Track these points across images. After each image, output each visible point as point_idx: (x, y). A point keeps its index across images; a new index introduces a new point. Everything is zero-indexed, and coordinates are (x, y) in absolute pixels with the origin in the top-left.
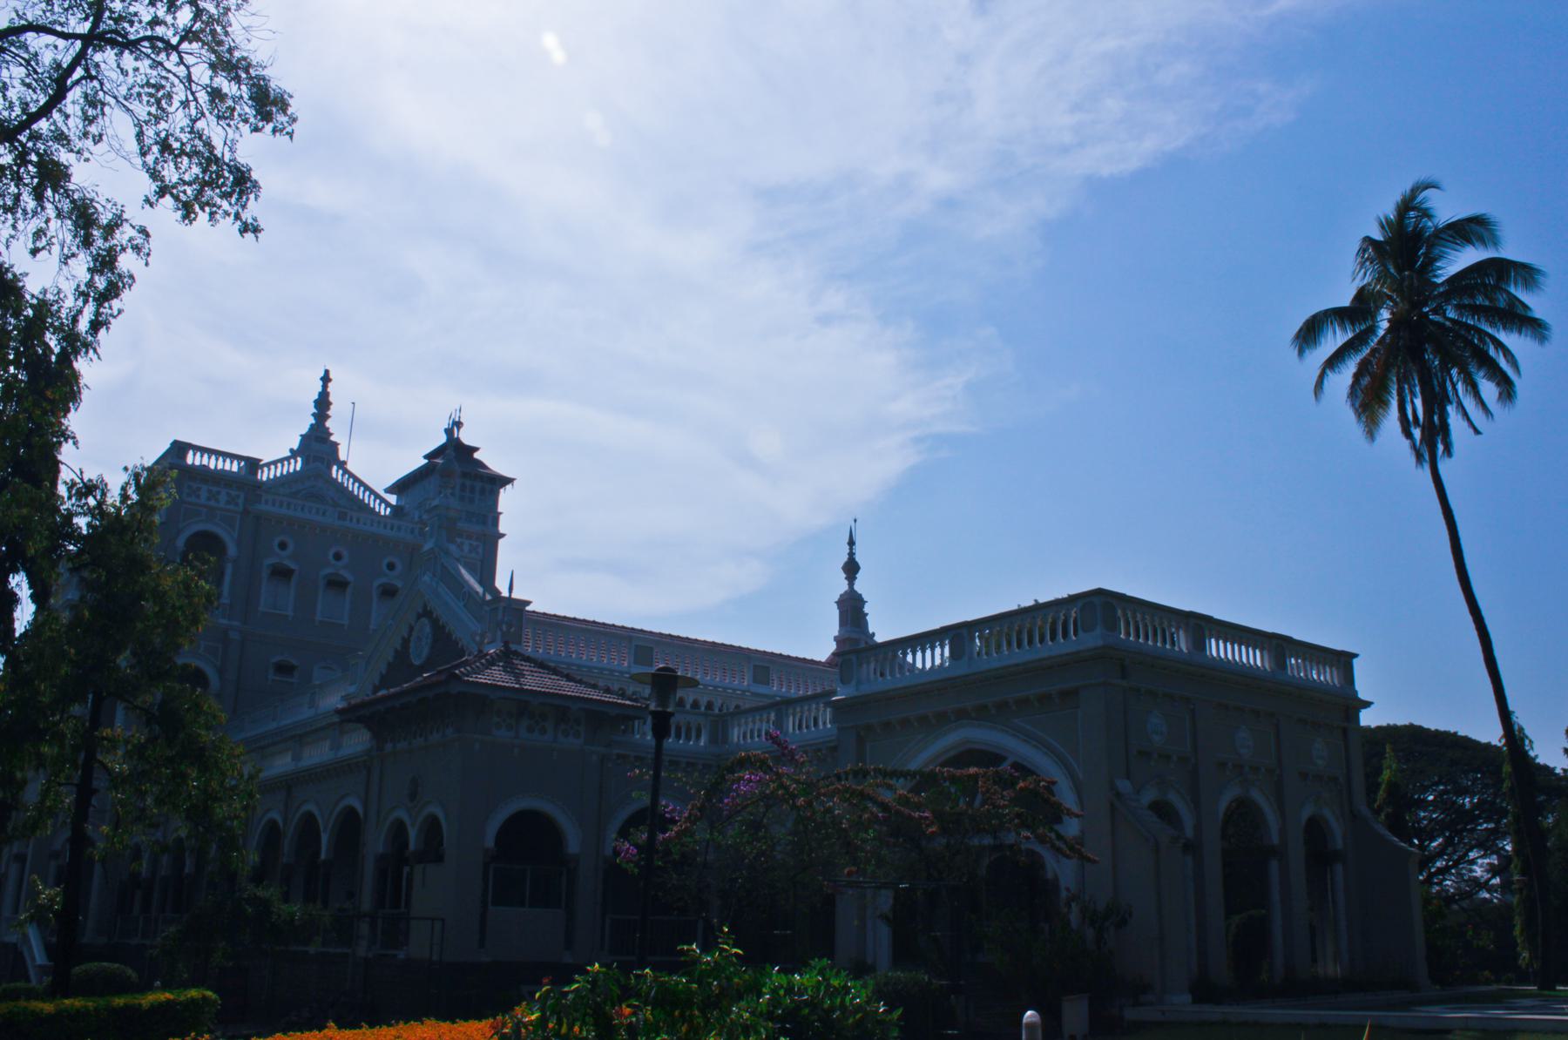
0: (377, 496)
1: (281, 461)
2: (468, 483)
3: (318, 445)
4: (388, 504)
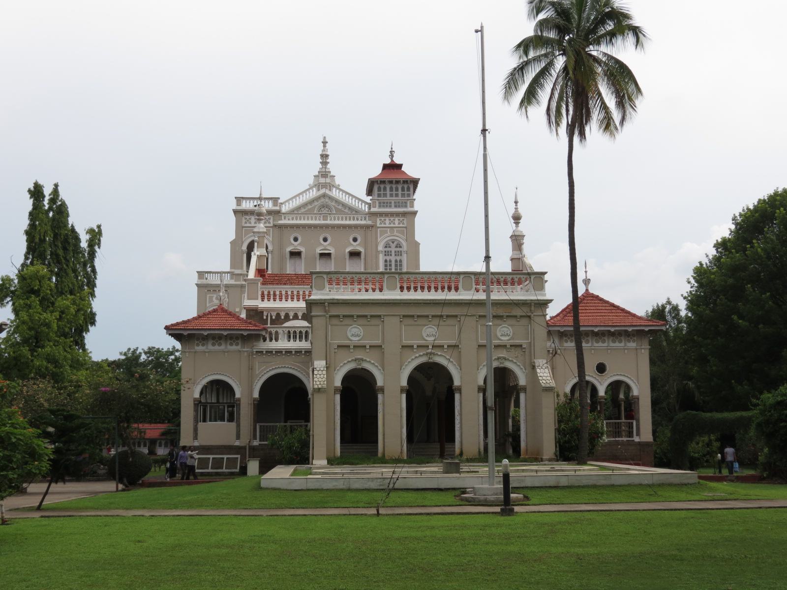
0: (359, 200)
1: (305, 191)
2: (394, 186)
3: (324, 177)
4: (366, 203)
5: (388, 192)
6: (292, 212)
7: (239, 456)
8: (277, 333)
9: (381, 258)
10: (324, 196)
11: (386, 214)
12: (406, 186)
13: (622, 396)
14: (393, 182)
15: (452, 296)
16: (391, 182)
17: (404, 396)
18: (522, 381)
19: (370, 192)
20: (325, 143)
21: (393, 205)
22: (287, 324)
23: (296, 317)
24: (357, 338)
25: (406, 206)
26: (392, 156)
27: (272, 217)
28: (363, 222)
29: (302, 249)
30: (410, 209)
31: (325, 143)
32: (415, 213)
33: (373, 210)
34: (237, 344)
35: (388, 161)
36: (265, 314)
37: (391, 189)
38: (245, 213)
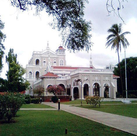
9: (60, 63)
10: (48, 51)
15: (89, 72)
18: (109, 86)
19: (56, 51)
28: (56, 57)
38: (35, 54)
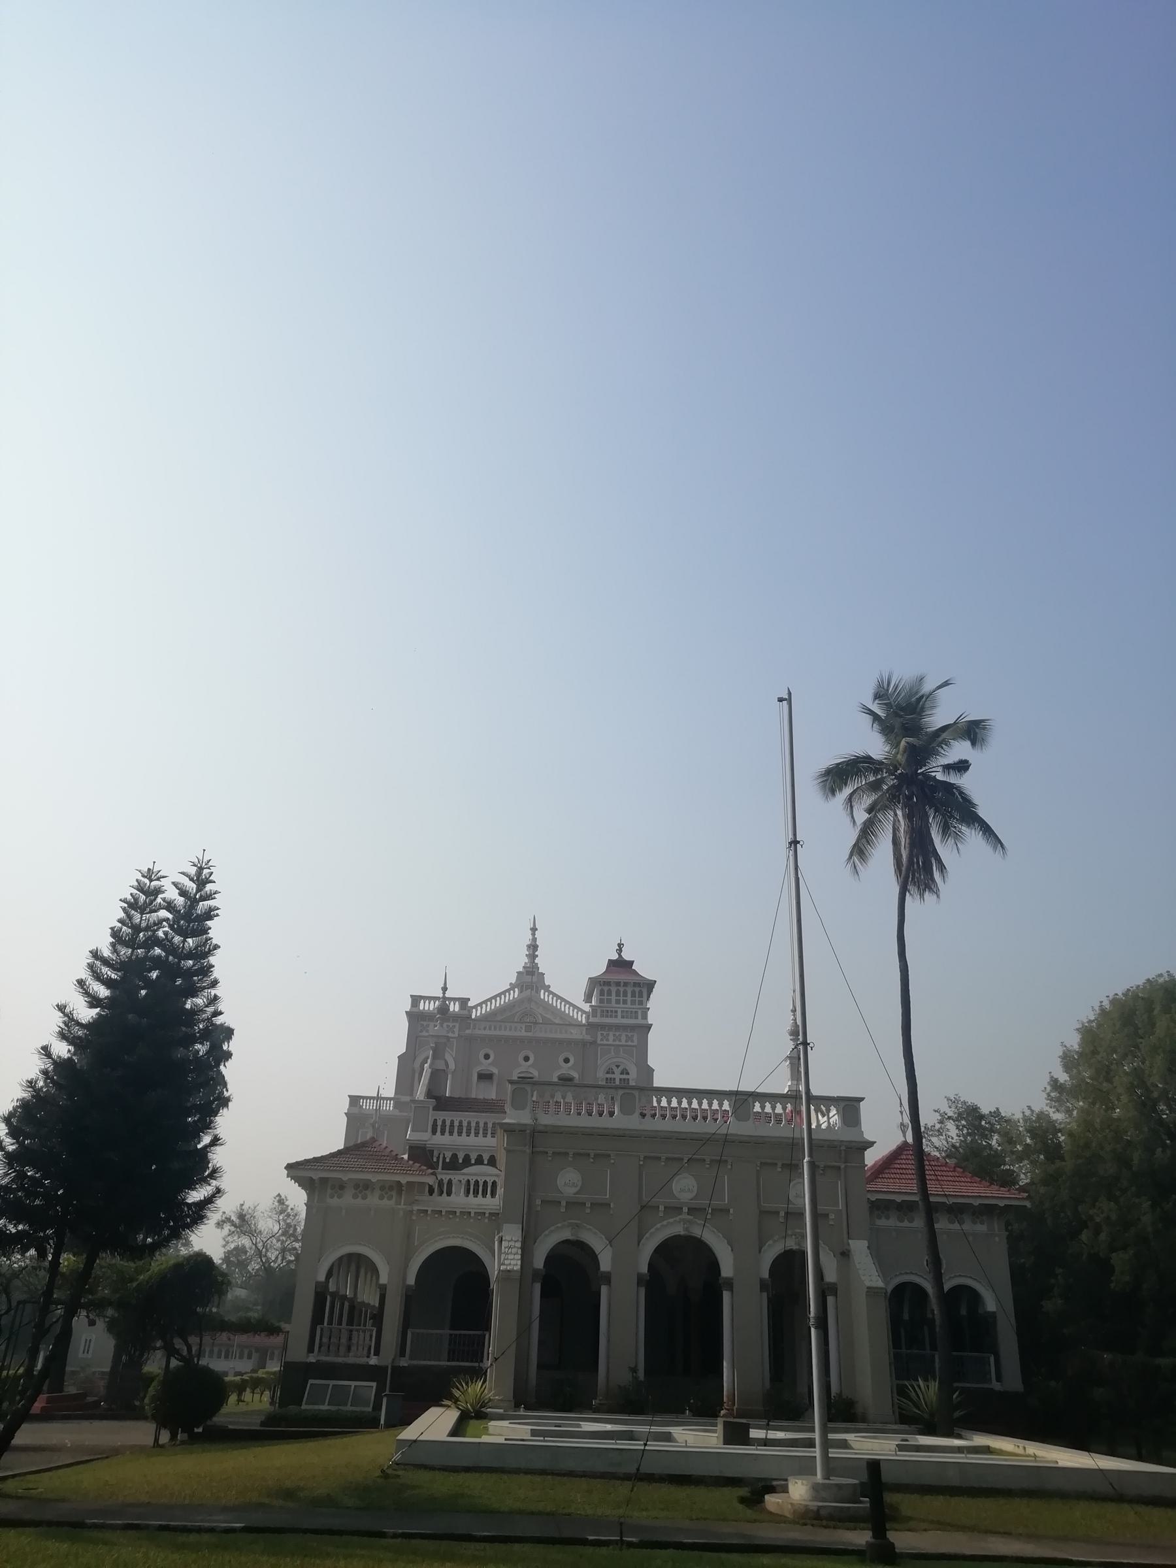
0: (575, 1007)
1: (504, 993)
2: (622, 989)
4: (583, 1012)
5: (614, 997)
6: (486, 1018)
7: (374, 1384)
8: (450, 1182)
10: (530, 1000)
11: (610, 1027)
12: (637, 989)
13: (964, 1312)
14: (622, 985)
16: (618, 984)
17: (642, 1291)
20: (534, 930)
21: (619, 1014)
22: (465, 1171)
23: (479, 1161)
24: (575, 1190)
25: (636, 1018)
26: (620, 950)
27: (457, 1025)
29: (495, 1071)
30: (643, 1022)
31: (534, 930)
32: (649, 1027)
33: (592, 1020)
34: (390, 1198)
35: (615, 957)
36: (436, 1154)
37: (618, 994)
